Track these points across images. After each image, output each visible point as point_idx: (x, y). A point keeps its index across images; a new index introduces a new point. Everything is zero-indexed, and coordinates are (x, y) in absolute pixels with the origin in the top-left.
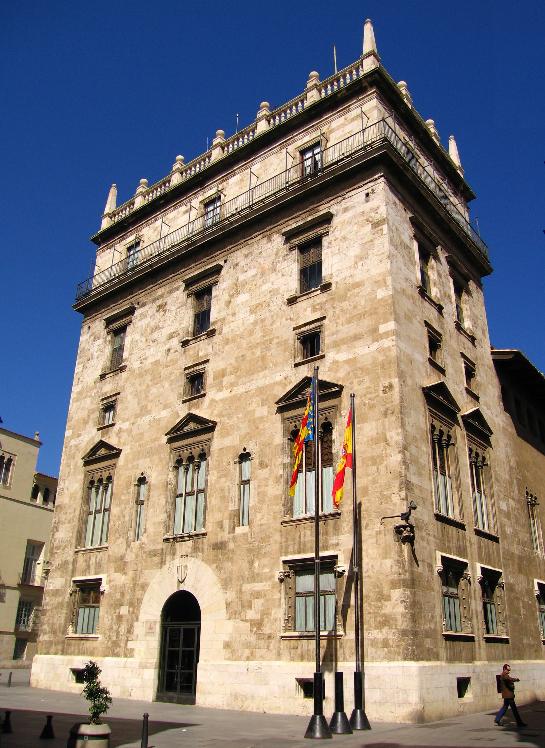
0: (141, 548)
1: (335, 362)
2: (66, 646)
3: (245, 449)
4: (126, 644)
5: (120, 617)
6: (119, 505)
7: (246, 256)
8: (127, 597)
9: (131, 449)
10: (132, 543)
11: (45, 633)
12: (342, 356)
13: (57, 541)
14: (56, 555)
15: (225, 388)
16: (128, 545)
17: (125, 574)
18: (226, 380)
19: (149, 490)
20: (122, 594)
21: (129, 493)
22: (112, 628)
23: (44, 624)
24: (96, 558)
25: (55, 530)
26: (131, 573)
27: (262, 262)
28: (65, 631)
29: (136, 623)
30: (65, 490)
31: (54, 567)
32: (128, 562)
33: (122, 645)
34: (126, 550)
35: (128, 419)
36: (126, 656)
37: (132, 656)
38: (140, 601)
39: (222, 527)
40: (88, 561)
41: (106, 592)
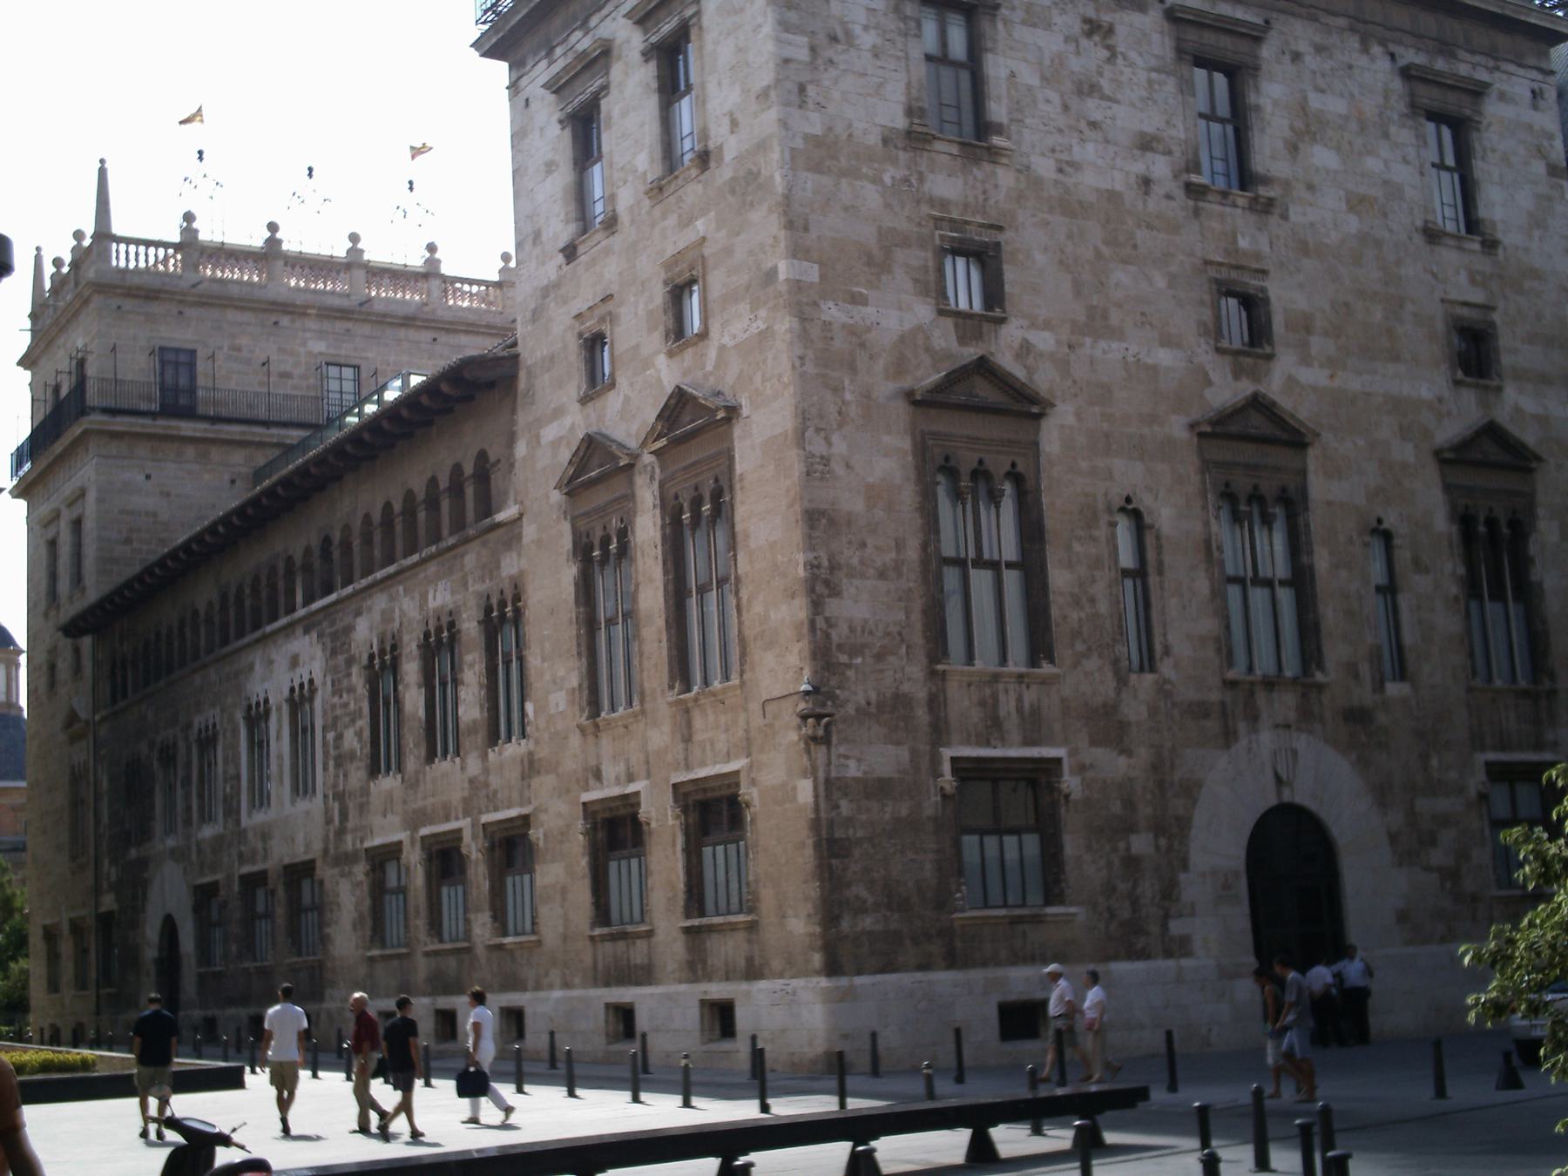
0: (1164, 690)
1: (1518, 410)
2: (959, 945)
3: (1380, 521)
4: (1165, 927)
5: (1132, 863)
6: (1070, 566)
7: (1319, 49)
8: (1145, 811)
9: (1078, 415)
10: (1133, 677)
11: (862, 910)
12: (1529, 404)
13: (844, 628)
14: (850, 673)
15: (1316, 364)
16: (1122, 681)
17: (1126, 752)
18: (1317, 343)
19: (1159, 548)
20: (1129, 804)
21: (1094, 539)
22: (1114, 889)
23: (849, 885)
24: (1020, 699)
25: (820, 588)
26: (1143, 754)
27: (1356, 92)
28: (942, 902)
29: (1182, 877)
30: (839, 469)
31: (850, 709)
32: (1129, 724)
33: (1154, 929)
34: (1118, 691)
35: (1047, 325)
36: (1168, 954)
37: (1188, 954)
38: (1184, 823)
39: (1356, 676)
40: (990, 707)
41: (1073, 797)
